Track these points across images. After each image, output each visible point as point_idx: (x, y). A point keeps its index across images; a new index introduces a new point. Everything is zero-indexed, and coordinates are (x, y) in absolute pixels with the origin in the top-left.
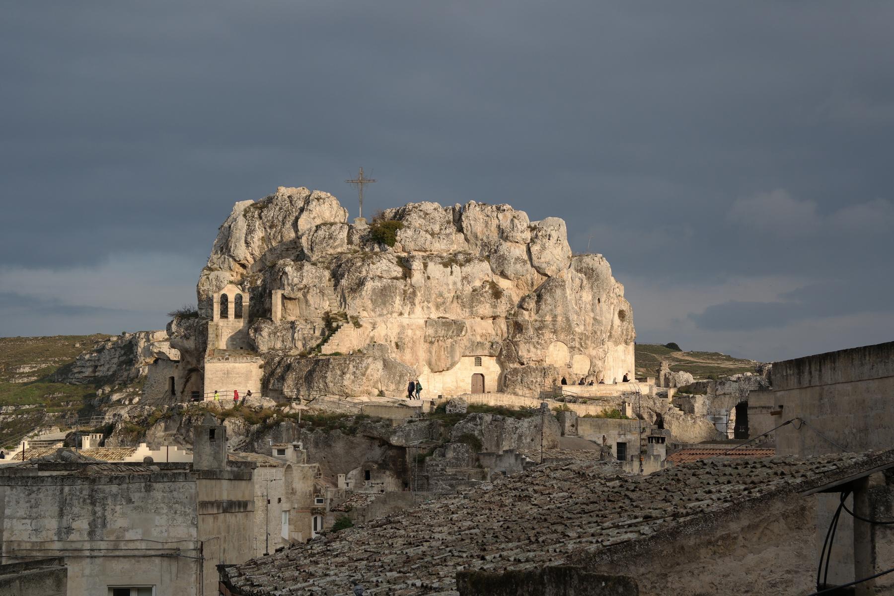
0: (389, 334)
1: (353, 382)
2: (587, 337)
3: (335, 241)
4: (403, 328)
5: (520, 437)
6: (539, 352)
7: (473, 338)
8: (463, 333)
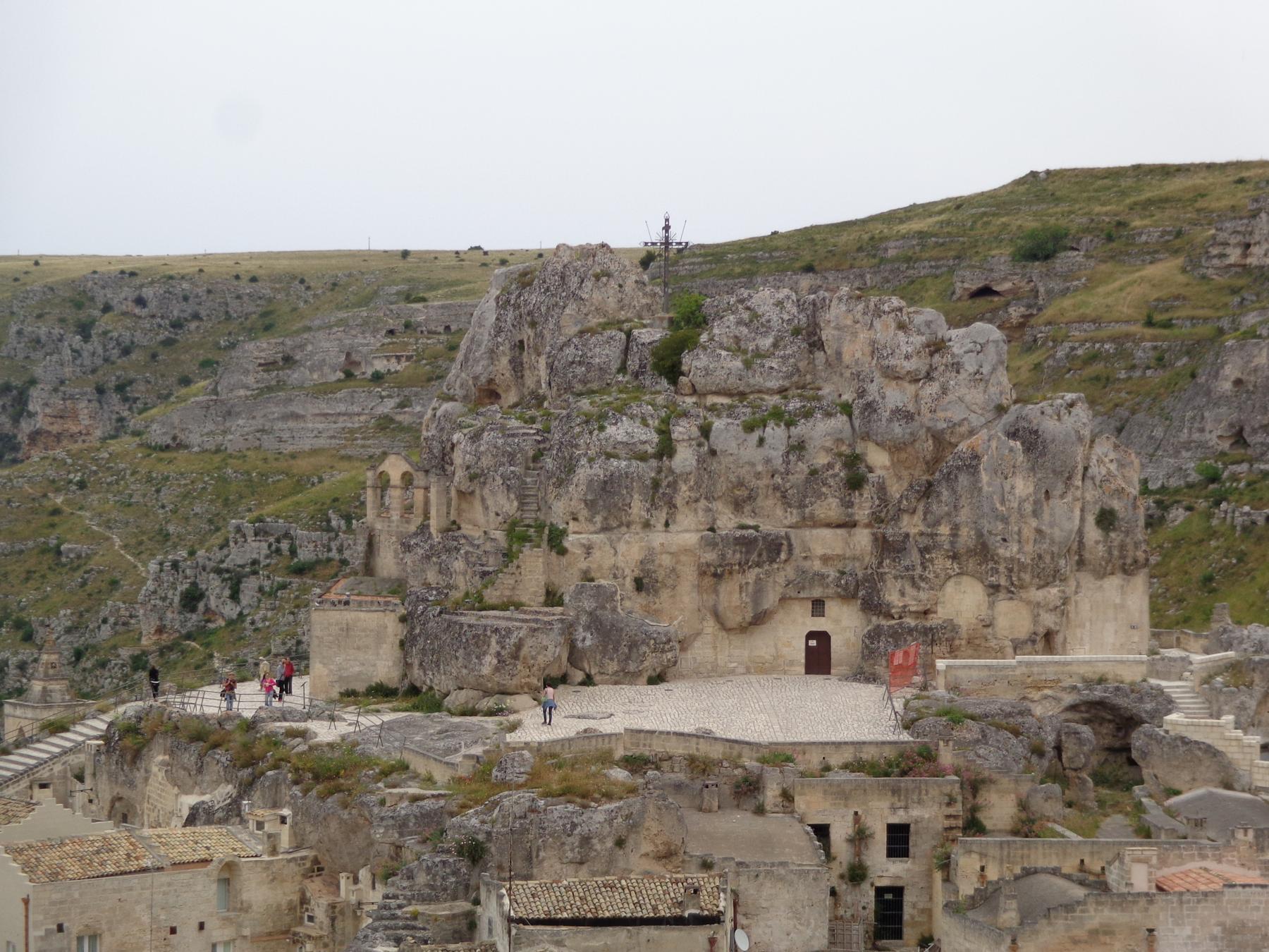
1: (497, 669)
2: (1023, 567)
6: (923, 595)
7: (807, 564)
8: (783, 556)
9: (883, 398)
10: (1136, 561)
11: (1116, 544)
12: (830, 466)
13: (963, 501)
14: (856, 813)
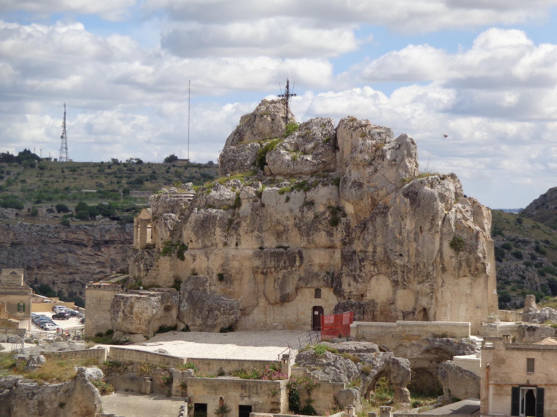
0: (211, 266)
3: (235, 164)
4: (227, 259)
5: (41, 403)
6: (360, 286)
8: (297, 263)
9: (350, 175)
10: (477, 269)
11: (463, 258)
12: (324, 213)
13: (379, 233)
14: (221, 398)
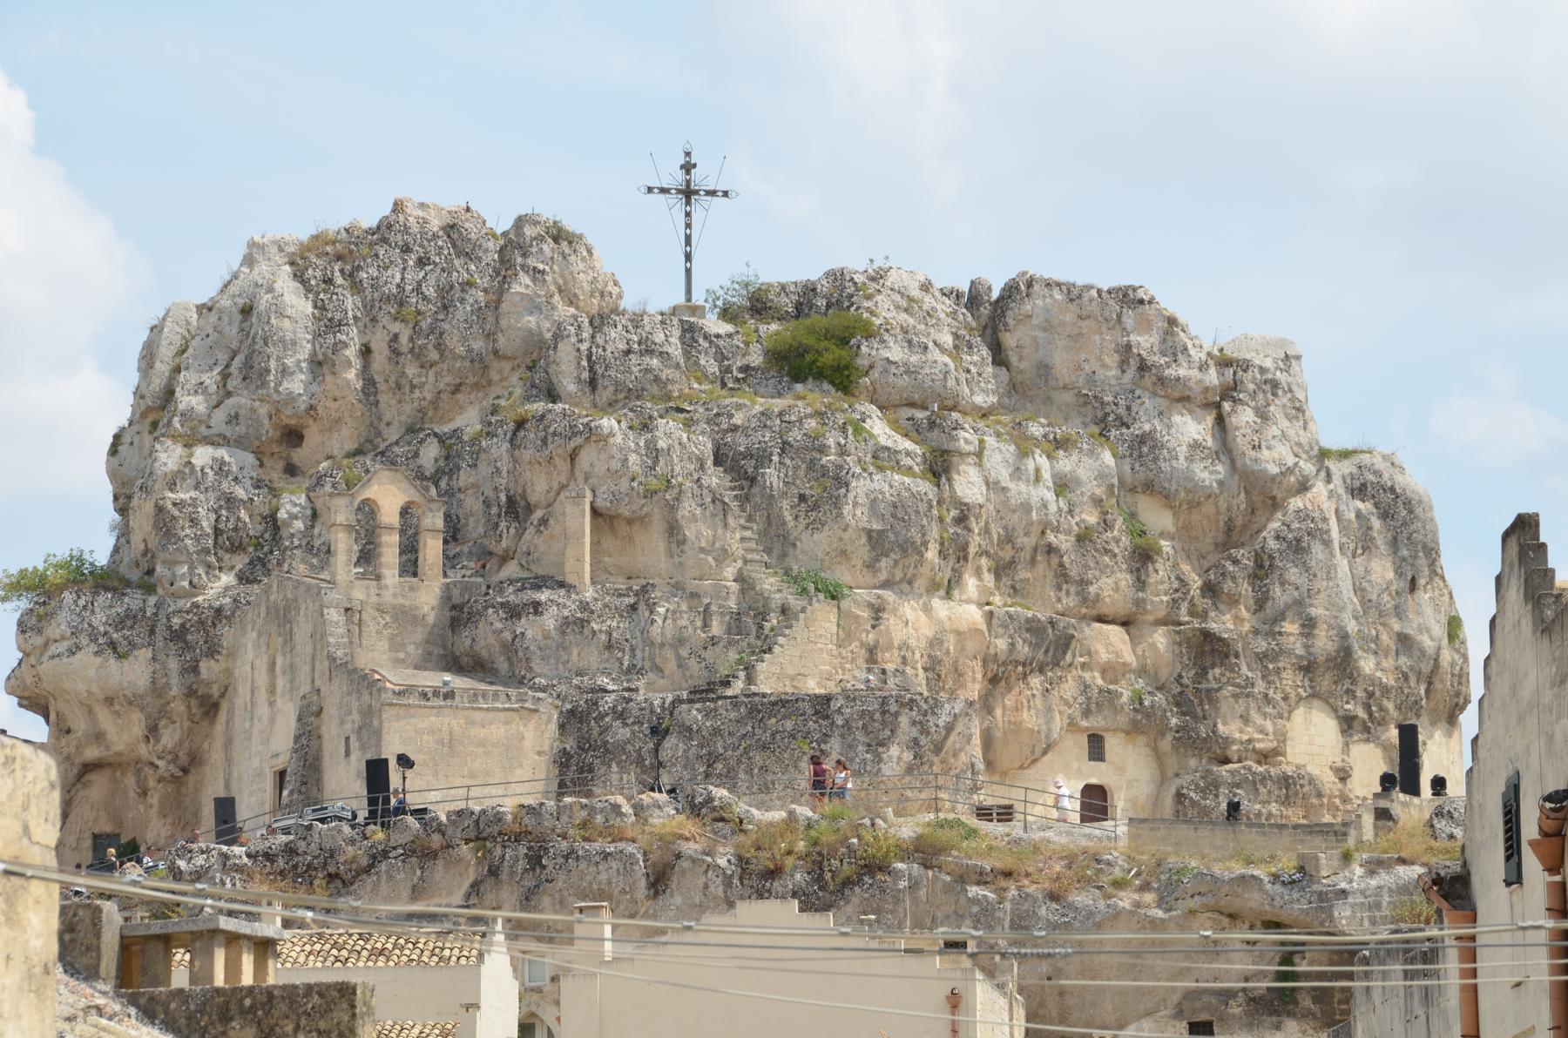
1: (909, 770)
